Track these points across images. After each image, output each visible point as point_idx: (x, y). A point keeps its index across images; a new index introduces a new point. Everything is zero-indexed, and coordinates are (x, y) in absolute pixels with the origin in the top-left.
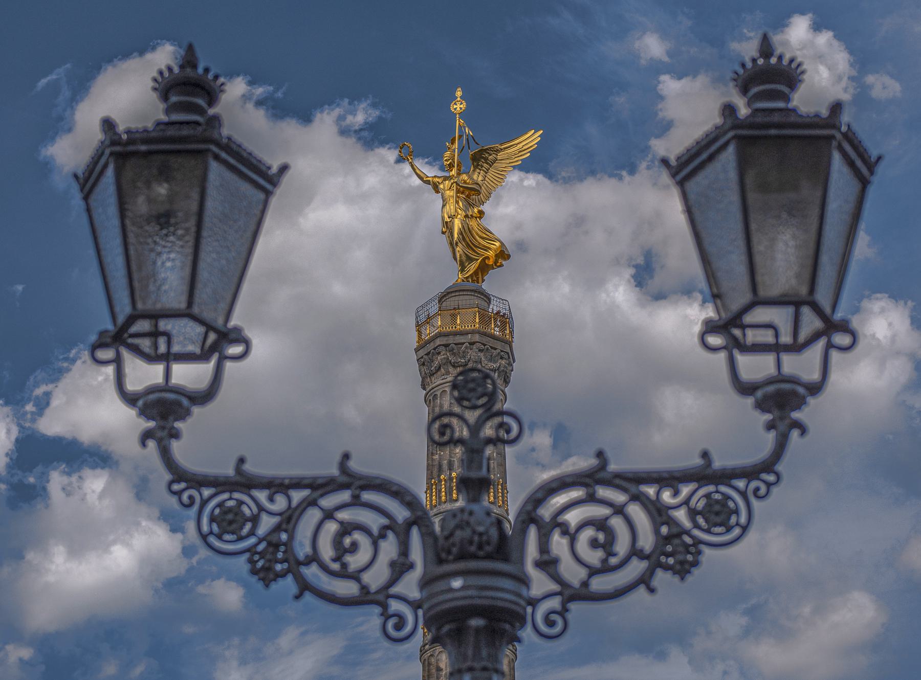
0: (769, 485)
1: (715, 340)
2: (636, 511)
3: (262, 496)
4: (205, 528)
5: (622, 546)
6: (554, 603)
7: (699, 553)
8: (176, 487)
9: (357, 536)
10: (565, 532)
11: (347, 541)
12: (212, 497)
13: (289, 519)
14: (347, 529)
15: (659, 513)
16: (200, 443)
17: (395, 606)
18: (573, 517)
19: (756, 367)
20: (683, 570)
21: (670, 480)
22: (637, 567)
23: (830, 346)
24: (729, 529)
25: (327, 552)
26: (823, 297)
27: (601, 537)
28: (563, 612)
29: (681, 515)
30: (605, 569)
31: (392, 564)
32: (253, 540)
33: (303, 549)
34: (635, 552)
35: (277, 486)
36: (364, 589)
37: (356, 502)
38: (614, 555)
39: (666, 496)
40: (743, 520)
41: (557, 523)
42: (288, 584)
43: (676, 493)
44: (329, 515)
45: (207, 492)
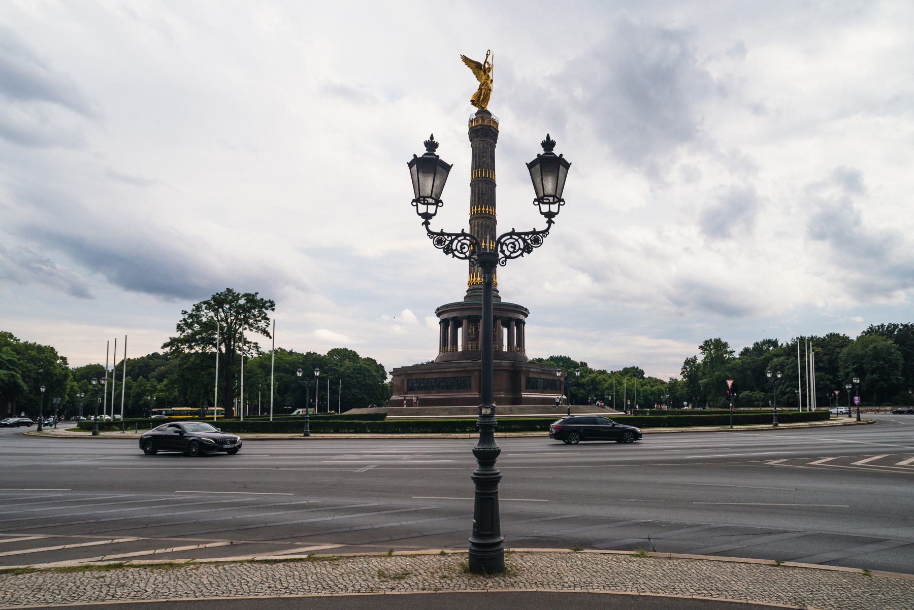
1: (536, 203)
2: (520, 240)
5: (517, 248)
13: (452, 242)
14: (463, 244)
15: (524, 241)
18: (507, 242)
19: (545, 208)
20: (529, 252)
21: (527, 234)
22: (520, 252)
25: (459, 249)
29: (529, 241)
30: (514, 252)
33: (454, 248)
34: (520, 249)
35: (449, 235)
37: (465, 239)
41: (504, 243)
42: (451, 255)
44: (459, 241)
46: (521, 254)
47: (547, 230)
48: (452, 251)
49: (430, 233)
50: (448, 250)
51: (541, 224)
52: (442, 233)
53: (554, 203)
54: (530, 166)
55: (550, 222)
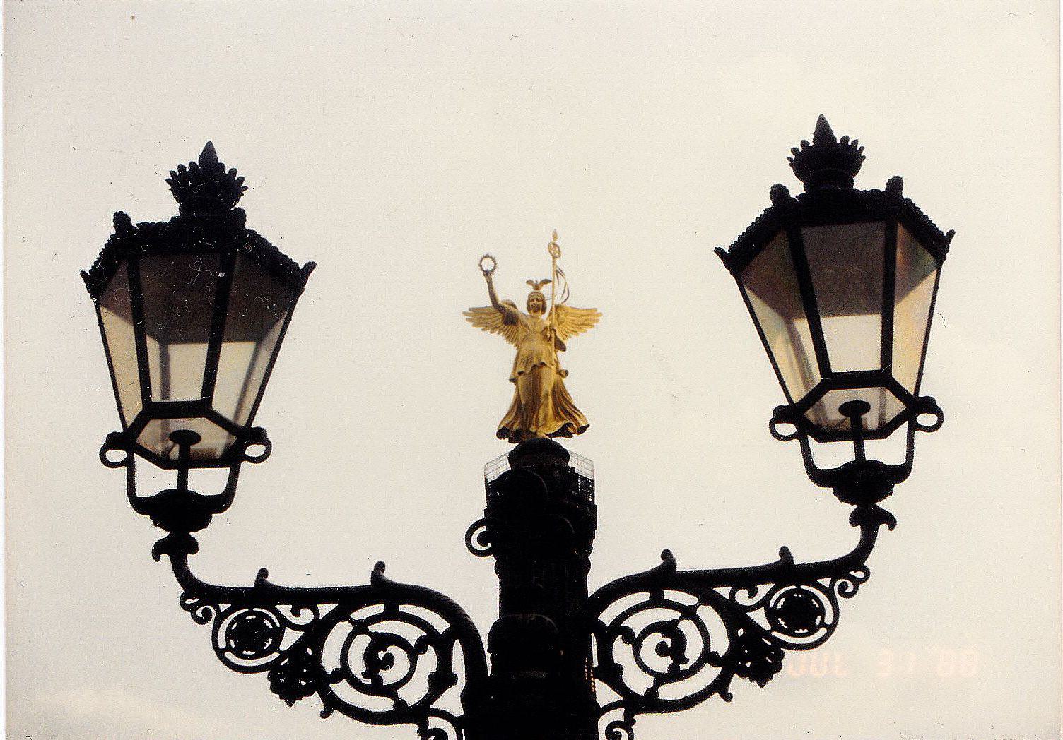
0: (857, 582)
1: (787, 429)
2: (708, 614)
3: (285, 610)
4: (222, 644)
5: (693, 651)
6: (618, 715)
7: (782, 655)
8: (189, 602)
9: (393, 650)
10: (628, 636)
11: (381, 655)
12: (227, 613)
13: (316, 633)
14: (382, 641)
15: (733, 615)
16: (223, 557)
17: (434, 723)
18: (636, 623)
21: (746, 578)
22: (710, 673)
24: (813, 630)
25: (358, 667)
27: (669, 642)
28: (628, 724)
29: (759, 617)
30: (674, 675)
31: (433, 679)
32: (276, 655)
33: (330, 661)
34: (708, 657)
35: (302, 598)
36: (400, 704)
37: (391, 614)
38: (686, 661)
39: (742, 597)
40: (829, 620)
41: (618, 628)
42: (314, 702)
43: (753, 593)
44: (360, 627)
45: (223, 607)
46: (720, 687)
48: (320, 682)
49: (199, 596)
50: (297, 677)
51: (825, 530)
52: (264, 593)
54: (740, 258)
55: (870, 520)
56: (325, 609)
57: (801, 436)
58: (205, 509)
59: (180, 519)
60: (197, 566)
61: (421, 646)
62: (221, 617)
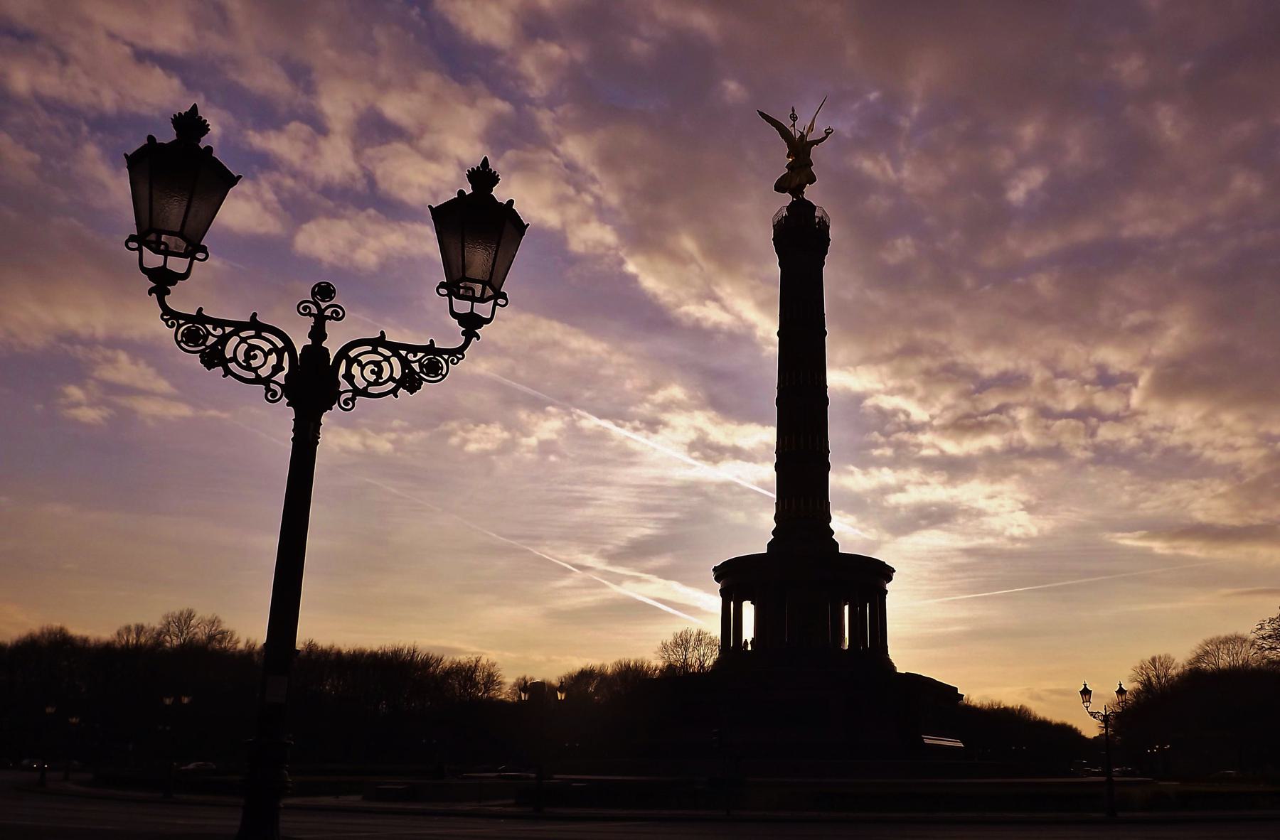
0: (459, 359)
2: (394, 360)
5: (385, 375)
6: (350, 395)
9: (257, 352)
10: (360, 363)
13: (224, 339)
15: (405, 363)
16: (182, 299)
17: (273, 386)
19: (463, 306)
22: (391, 385)
23: (496, 304)
25: (241, 358)
26: (495, 282)
28: (353, 399)
29: (416, 366)
30: (376, 383)
33: (229, 354)
34: (391, 378)
36: (258, 376)
37: (258, 336)
39: (411, 357)
42: (219, 370)
44: (243, 340)
46: (394, 392)
47: (461, 350)
48: (224, 362)
50: (213, 358)
52: (200, 318)
53: (483, 300)
55: (470, 334)
56: (228, 330)
57: (449, 295)
58: (175, 278)
59: (162, 281)
60: (168, 300)
61: (270, 352)
62: (180, 326)
